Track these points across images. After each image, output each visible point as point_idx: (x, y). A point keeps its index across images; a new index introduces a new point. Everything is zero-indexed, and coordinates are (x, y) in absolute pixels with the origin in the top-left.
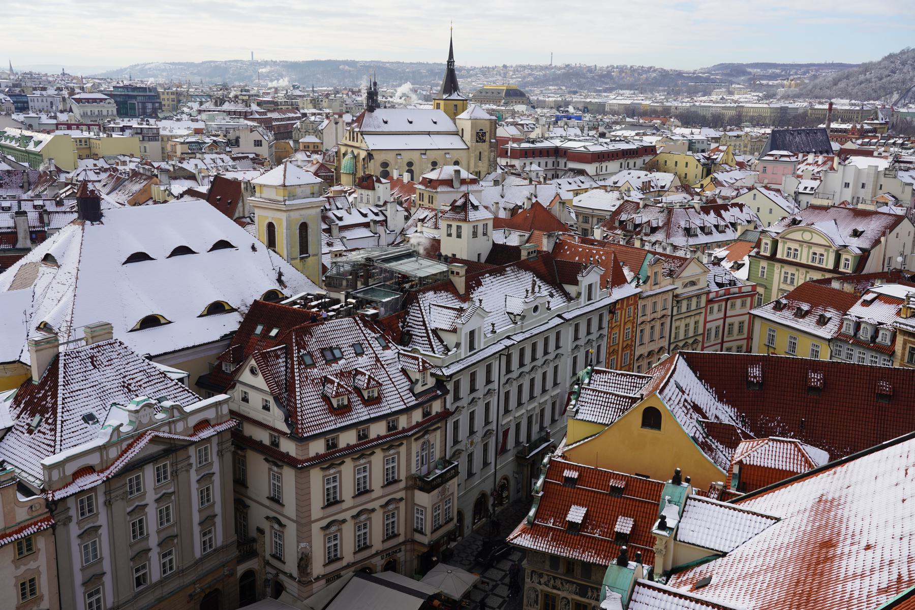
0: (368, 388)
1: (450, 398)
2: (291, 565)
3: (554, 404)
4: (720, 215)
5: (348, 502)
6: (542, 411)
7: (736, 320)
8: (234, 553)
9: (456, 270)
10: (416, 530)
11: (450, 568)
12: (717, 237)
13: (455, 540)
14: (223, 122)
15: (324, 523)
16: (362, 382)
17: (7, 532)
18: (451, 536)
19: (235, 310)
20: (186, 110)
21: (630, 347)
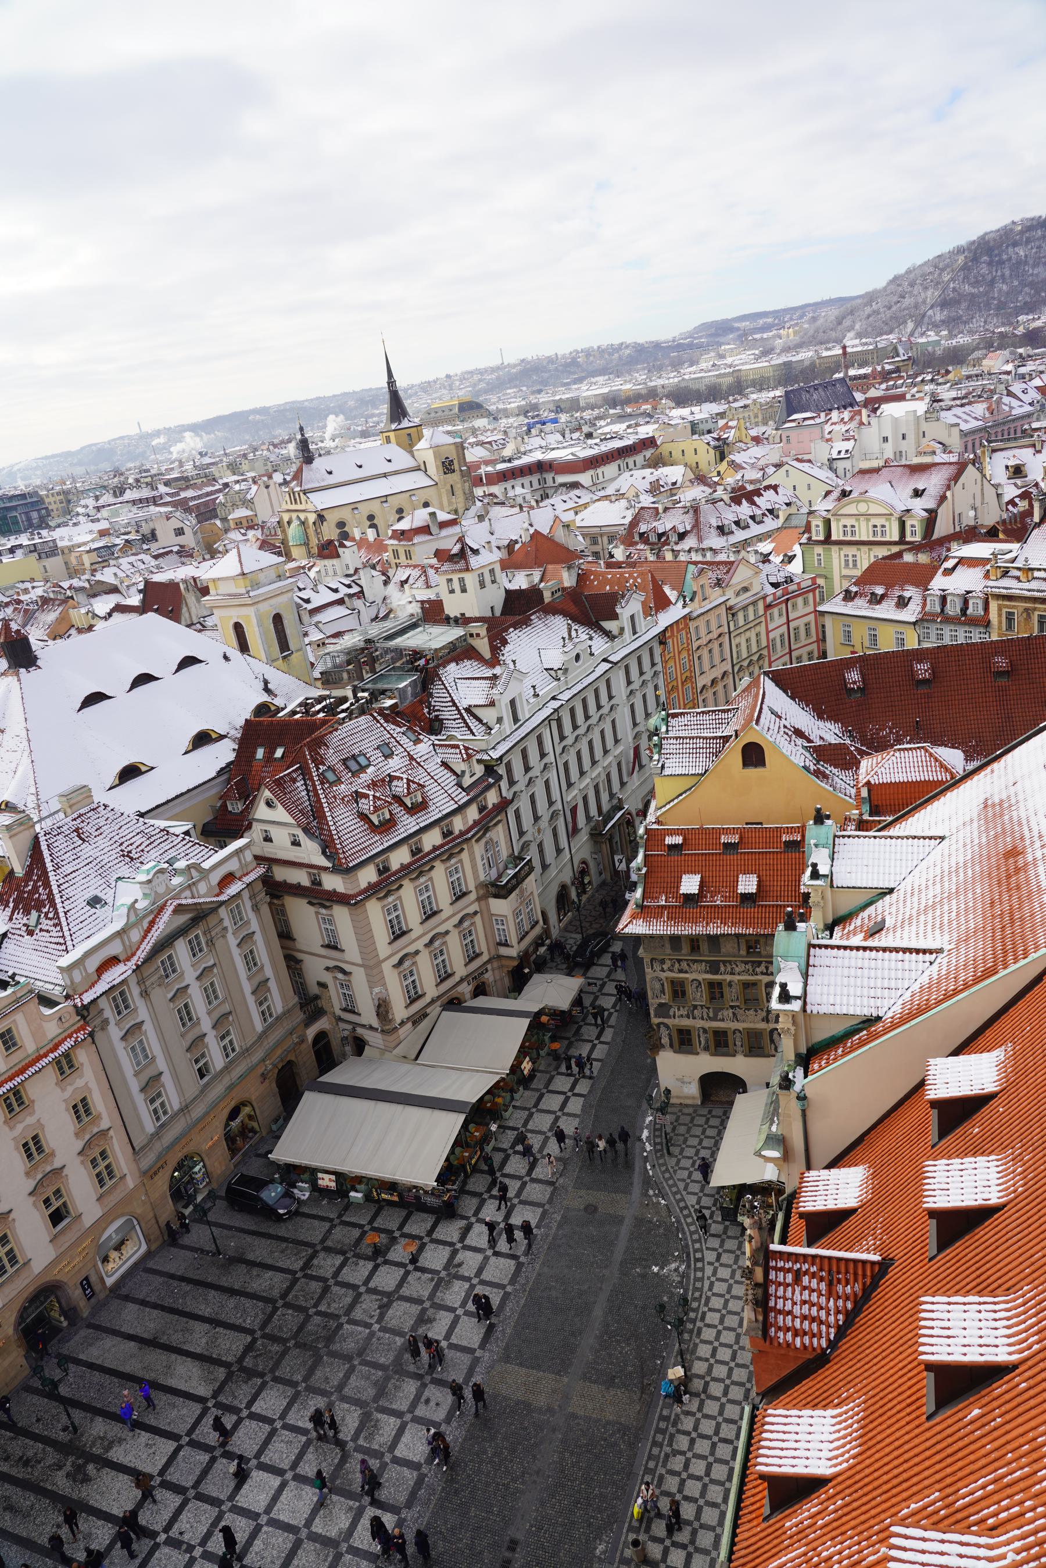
0: (409, 793)
1: (504, 784)
2: (368, 1015)
3: (619, 764)
4: (753, 503)
5: (417, 930)
6: (608, 775)
7: (800, 623)
8: (299, 1016)
9: (474, 631)
10: (500, 944)
11: (548, 977)
12: (755, 529)
13: (543, 945)
14: (131, 515)
15: (395, 960)
16: (400, 788)
17: (42, 1052)
18: (538, 942)
19: (225, 737)
20: (80, 510)
21: (690, 679)
